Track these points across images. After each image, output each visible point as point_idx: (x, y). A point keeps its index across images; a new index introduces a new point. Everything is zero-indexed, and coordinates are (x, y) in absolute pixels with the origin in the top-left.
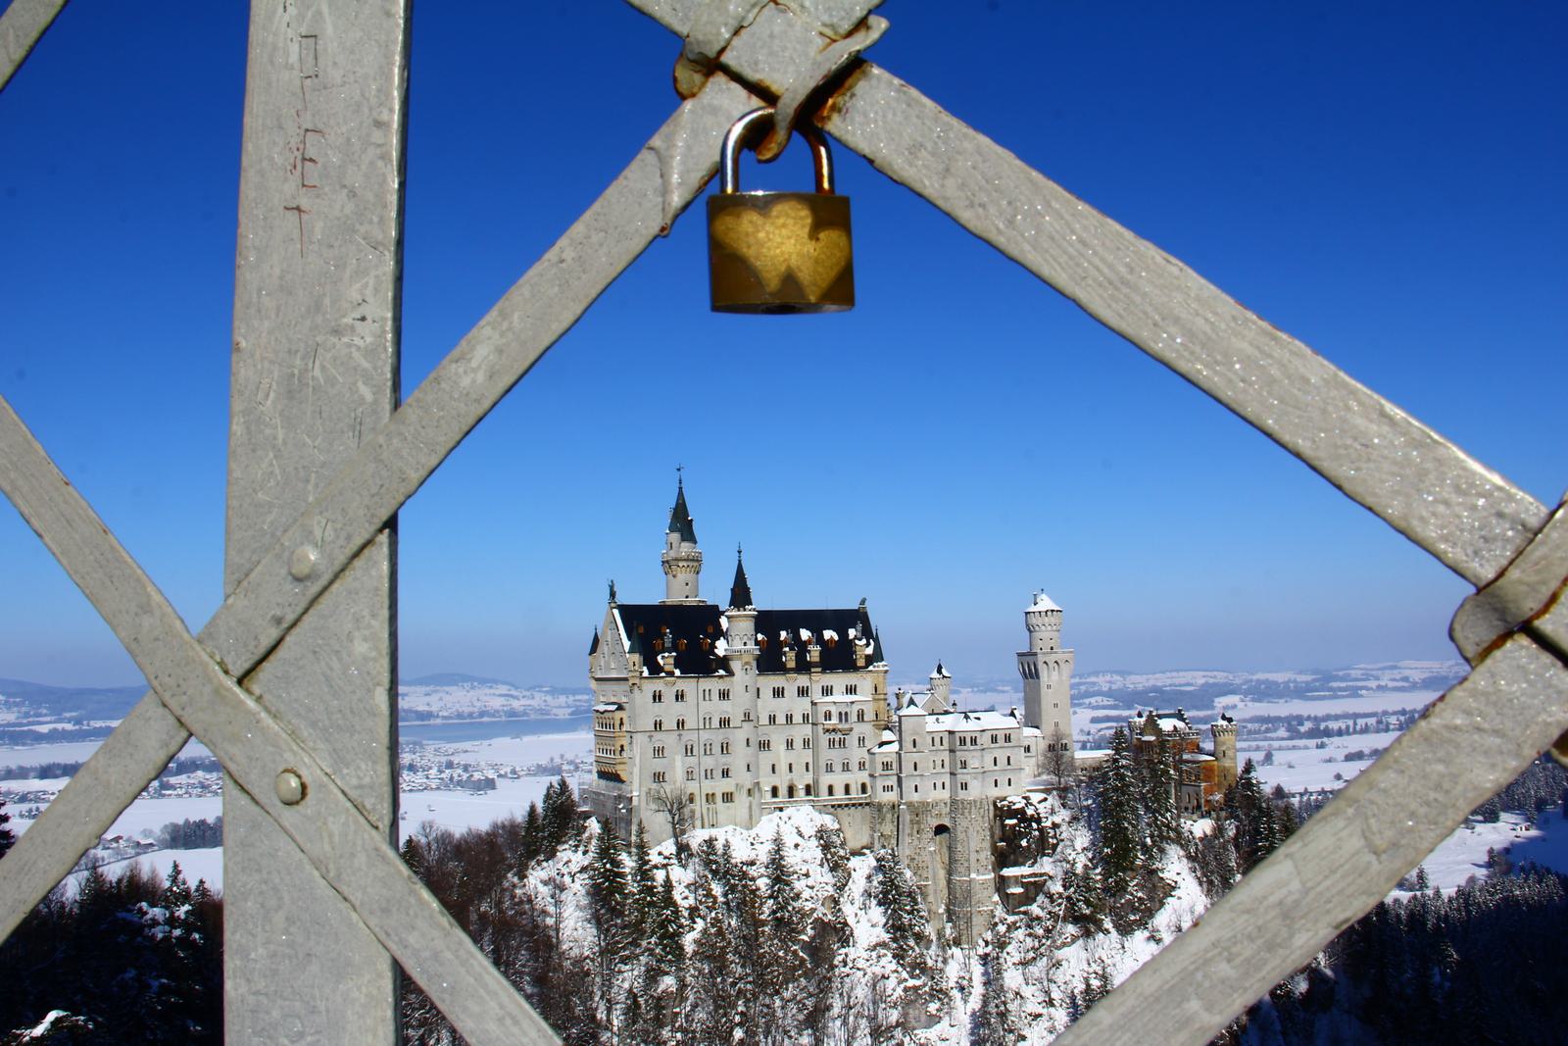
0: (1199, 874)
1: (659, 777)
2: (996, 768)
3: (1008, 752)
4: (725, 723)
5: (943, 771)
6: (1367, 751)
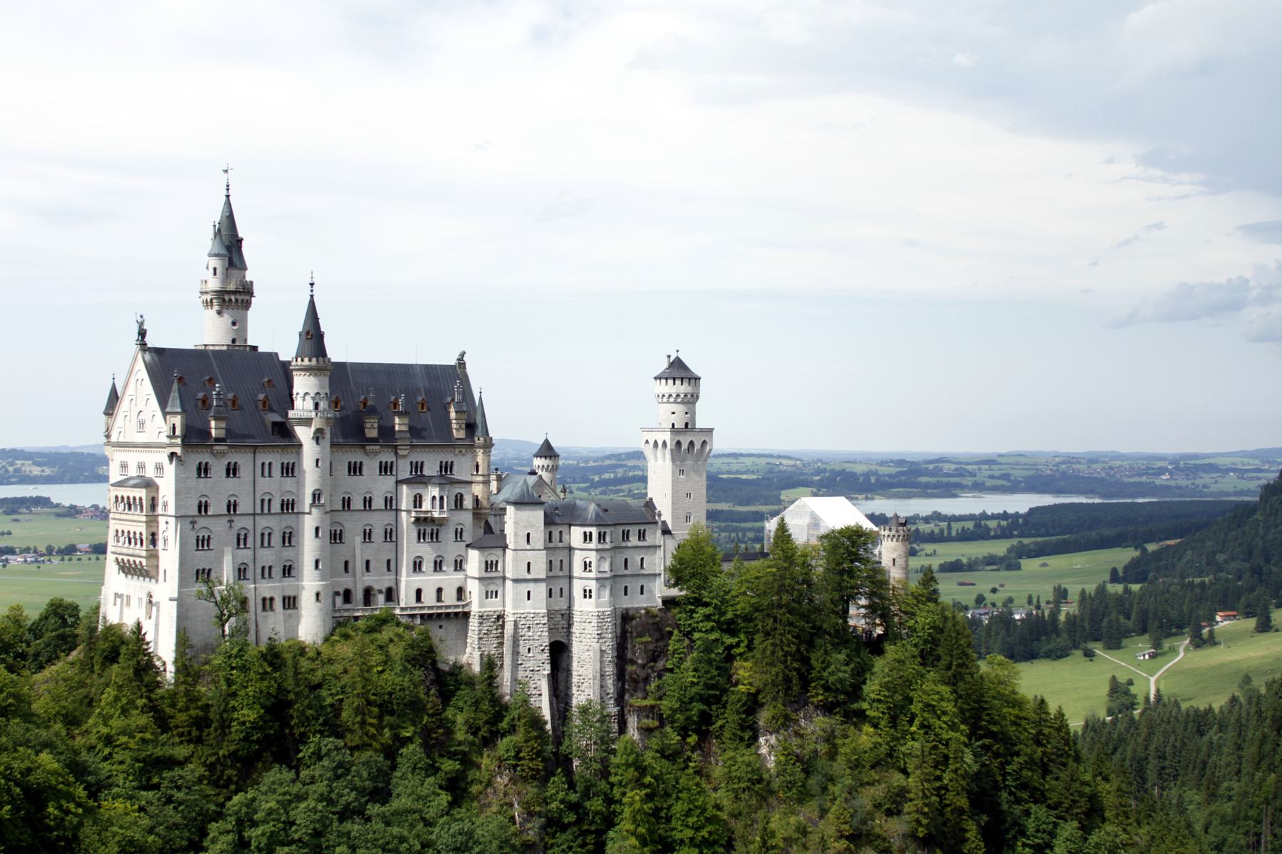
1: (204, 575)
6: (965, 560)
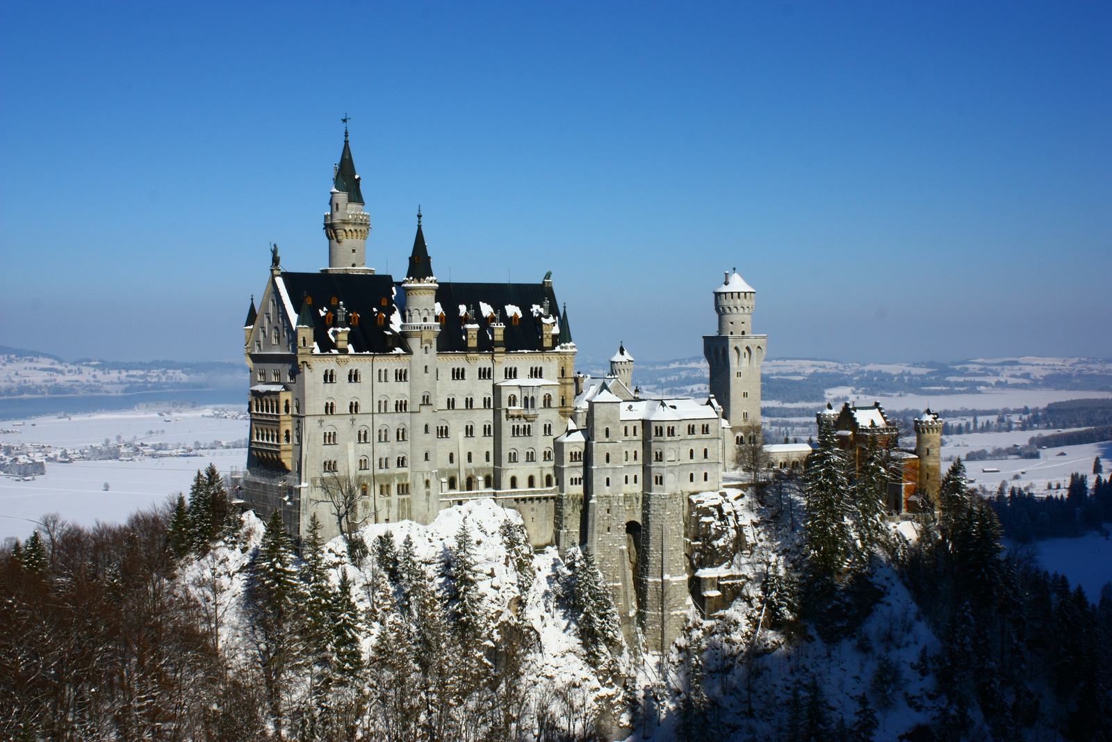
0: (907, 580)
1: (330, 466)
2: (692, 461)
3: (705, 445)
4: (401, 406)
5: (635, 463)
6: (990, 451)
